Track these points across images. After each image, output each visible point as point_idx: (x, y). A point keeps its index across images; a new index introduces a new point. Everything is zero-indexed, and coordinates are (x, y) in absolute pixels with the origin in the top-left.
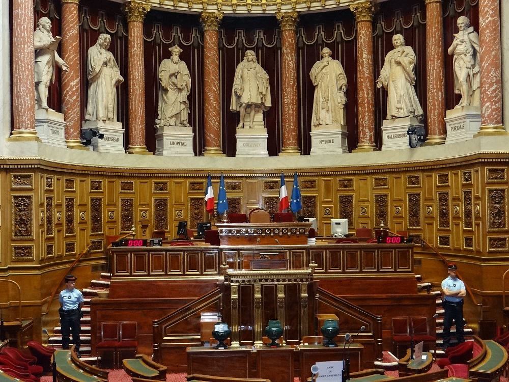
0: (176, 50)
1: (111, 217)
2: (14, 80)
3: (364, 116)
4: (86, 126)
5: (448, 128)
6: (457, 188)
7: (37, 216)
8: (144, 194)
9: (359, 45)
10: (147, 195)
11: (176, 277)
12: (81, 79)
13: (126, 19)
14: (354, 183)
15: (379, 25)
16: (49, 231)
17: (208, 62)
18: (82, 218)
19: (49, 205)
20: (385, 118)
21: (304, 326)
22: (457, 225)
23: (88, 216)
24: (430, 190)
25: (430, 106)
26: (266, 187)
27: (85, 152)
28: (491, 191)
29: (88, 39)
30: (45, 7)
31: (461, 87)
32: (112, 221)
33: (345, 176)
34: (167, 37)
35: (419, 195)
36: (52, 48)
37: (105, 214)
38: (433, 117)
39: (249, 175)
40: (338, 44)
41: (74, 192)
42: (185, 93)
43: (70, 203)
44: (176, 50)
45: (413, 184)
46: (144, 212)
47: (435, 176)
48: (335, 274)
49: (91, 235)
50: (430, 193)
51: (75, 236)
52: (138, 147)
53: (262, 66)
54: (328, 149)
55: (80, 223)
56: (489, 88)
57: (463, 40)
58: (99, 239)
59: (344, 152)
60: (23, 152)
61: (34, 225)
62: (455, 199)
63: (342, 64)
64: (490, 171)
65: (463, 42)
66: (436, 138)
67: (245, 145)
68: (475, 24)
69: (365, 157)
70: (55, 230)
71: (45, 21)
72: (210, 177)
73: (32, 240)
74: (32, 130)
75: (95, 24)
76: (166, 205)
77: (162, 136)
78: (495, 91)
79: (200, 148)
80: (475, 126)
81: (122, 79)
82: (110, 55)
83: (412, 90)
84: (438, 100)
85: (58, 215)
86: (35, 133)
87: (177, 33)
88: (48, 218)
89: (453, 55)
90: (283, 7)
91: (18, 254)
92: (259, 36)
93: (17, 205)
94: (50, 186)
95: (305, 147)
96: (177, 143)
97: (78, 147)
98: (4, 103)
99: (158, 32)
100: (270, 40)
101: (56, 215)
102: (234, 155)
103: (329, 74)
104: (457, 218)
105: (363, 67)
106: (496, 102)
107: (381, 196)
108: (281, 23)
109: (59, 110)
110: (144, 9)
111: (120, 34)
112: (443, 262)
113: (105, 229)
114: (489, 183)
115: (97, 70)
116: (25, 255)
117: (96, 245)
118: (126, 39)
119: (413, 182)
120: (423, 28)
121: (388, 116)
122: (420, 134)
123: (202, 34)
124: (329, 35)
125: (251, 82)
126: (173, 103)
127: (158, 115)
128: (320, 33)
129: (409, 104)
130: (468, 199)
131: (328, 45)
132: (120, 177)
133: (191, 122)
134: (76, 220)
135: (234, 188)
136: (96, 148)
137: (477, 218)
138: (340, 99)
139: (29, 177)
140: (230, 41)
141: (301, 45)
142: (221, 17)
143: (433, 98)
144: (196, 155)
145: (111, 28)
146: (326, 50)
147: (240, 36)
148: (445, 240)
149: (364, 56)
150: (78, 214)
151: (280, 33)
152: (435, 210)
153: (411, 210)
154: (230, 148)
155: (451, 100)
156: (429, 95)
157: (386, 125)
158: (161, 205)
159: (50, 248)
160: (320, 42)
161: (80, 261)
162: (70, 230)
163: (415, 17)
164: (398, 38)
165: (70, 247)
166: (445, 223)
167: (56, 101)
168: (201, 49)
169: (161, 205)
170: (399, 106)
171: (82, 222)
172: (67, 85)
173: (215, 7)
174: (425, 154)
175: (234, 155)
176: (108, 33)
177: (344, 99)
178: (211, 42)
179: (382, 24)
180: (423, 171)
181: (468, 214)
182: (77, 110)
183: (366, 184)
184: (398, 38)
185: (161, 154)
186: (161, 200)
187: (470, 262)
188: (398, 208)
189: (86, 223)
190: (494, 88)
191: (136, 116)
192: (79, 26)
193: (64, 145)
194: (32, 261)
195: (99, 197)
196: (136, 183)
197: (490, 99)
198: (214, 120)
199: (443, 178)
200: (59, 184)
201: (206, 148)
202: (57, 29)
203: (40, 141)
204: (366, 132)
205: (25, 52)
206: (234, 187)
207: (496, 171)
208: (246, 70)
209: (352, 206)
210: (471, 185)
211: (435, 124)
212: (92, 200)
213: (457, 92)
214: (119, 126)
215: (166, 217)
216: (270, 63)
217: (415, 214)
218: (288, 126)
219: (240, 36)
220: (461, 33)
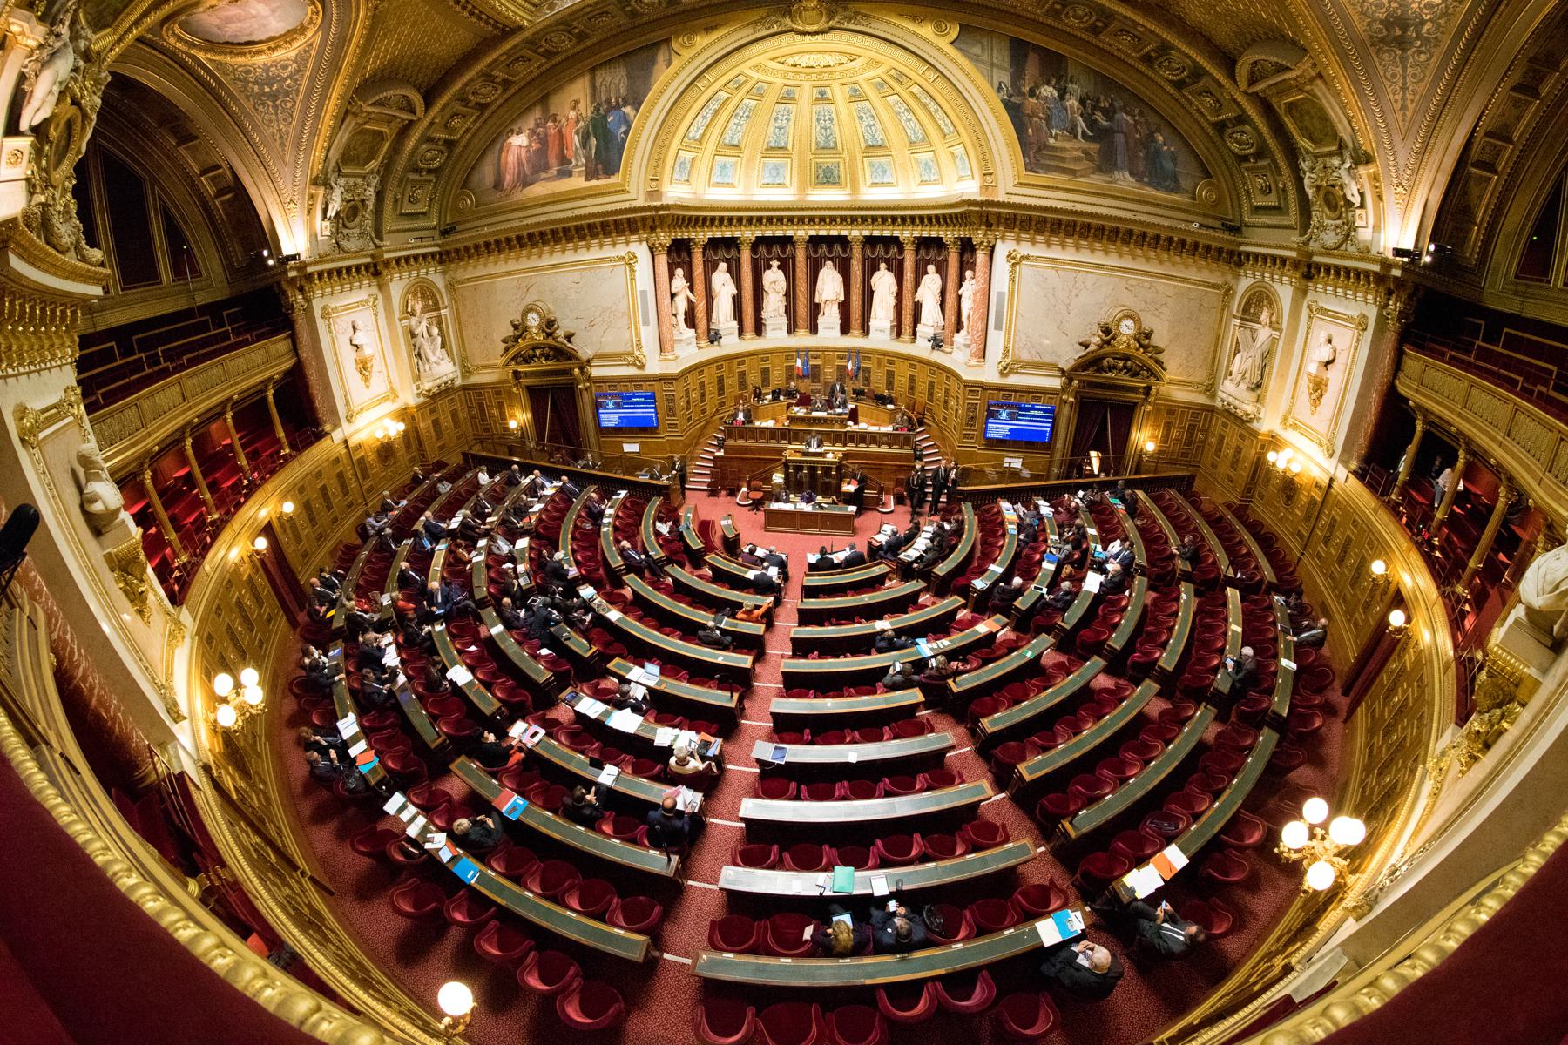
0: (775, 264)
3: (907, 317)
31: (964, 319)
33: (893, 357)
34: (769, 252)
37: (727, 382)
39: (824, 350)
43: (702, 385)
44: (775, 264)
52: (749, 334)
57: (968, 289)
66: (947, 348)
69: (904, 347)
71: (679, 272)
85: (694, 396)
87: (776, 249)
92: (837, 248)
95: (866, 330)
99: (762, 250)
100: (844, 251)
122: (937, 343)
125: (830, 284)
126: (774, 304)
131: (887, 262)
138: (893, 301)
140: (815, 252)
146: (883, 266)
147: (823, 248)
154: (814, 329)
155: (959, 326)
157: (920, 328)
158: (765, 372)
163: (944, 253)
164: (931, 268)
165: (704, 411)
167: (691, 321)
168: (794, 258)
174: (937, 357)
178: (801, 255)
179: (923, 251)
184: (931, 268)
188: (922, 387)
198: (802, 310)
202: (689, 277)
204: (907, 329)
214: (735, 324)
216: (844, 270)
217: (931, 394)
218: (854, 316)
219: (823, 248)
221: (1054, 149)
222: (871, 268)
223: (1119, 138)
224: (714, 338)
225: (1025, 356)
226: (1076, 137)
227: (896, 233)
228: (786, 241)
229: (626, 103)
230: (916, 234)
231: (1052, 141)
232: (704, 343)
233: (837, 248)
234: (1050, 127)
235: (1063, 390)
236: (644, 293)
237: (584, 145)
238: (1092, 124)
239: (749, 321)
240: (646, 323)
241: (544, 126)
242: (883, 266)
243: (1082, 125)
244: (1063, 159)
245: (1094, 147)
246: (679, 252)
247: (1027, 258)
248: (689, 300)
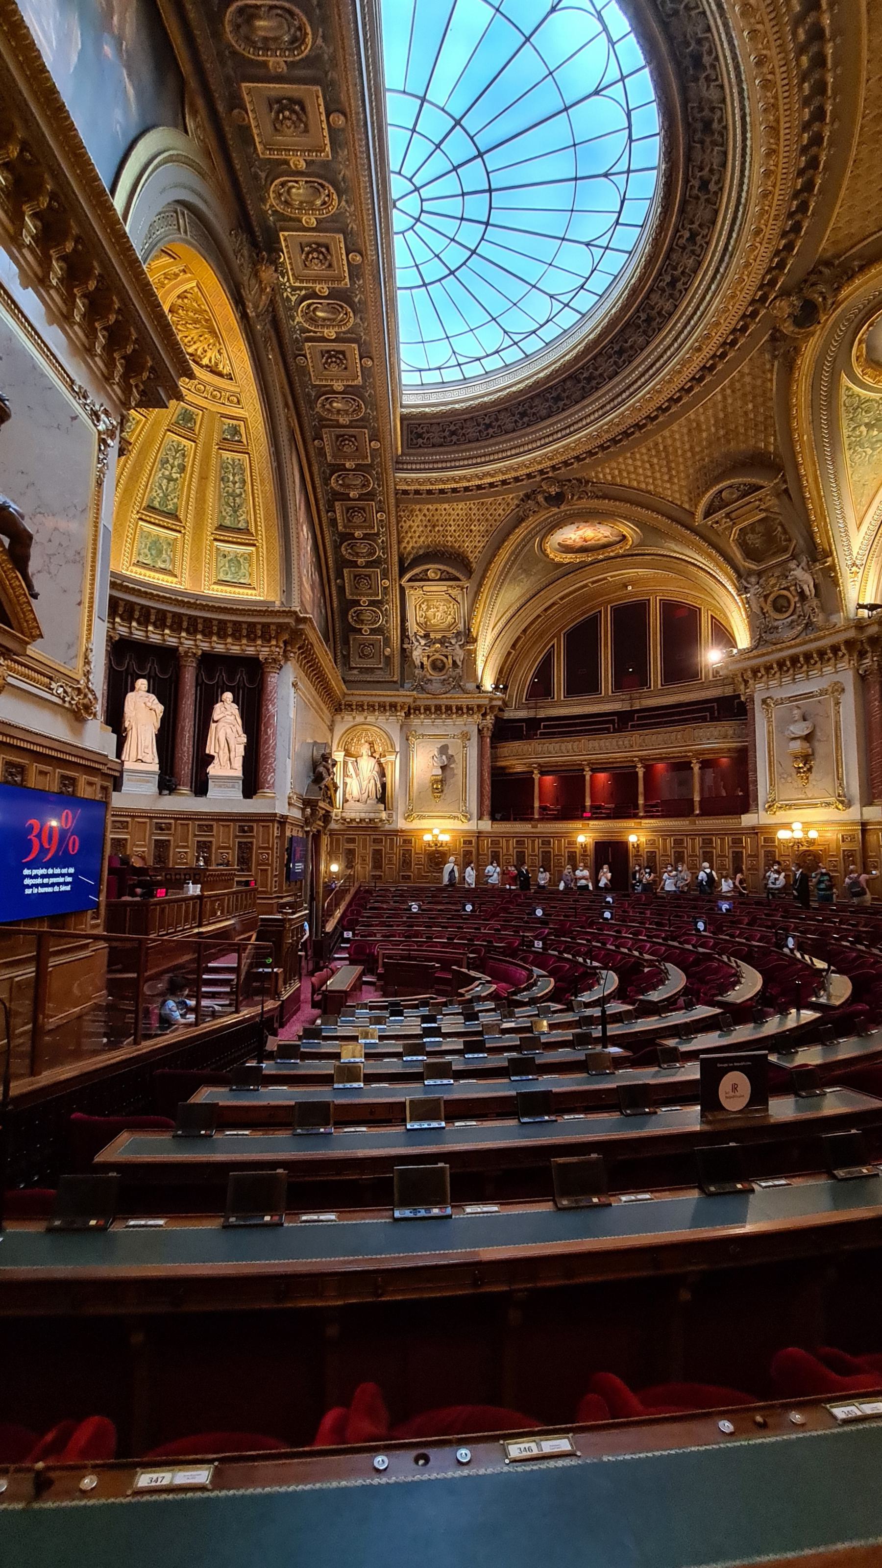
210: (253, 837)
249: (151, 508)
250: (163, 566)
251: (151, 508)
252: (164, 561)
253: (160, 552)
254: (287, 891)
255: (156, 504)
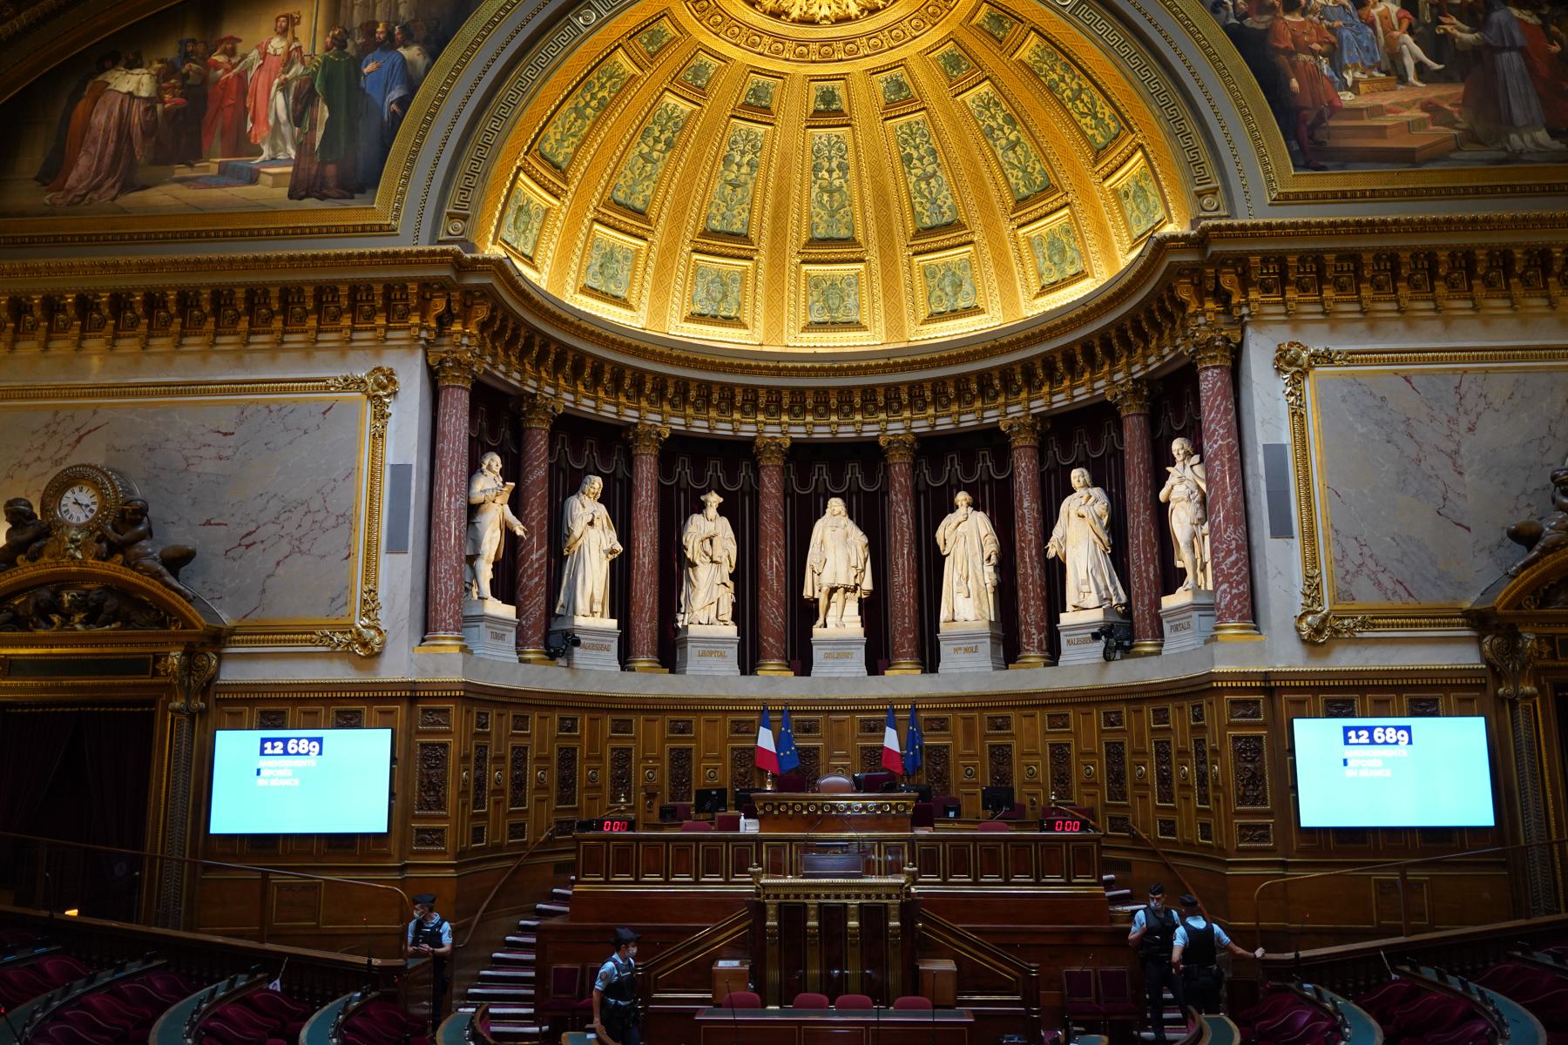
1: (591, 779)
2: (433, 553)
4: (556, 626)
5: (1166, 627)
6: (1183, 732)
7: (456, 776)
8: (649, 742)
9: (1016, 486)
10: (657, 744)
11: (681, 885)
12: (549, 551)
13: (630, 451)
14: (1013, 721)
15: (1050, 453)
16: (479, 802)
17: (765, 517)
18: (539, 780)
19: (481, 759)
20: (1064, 611)
21: (894, 977)
22: (1187, 799)
23: (551, 777)
24: (1141, 735)
25: (1135, 588)
26: (863, 729)
27: (550, 668)
28: (1236, 739)
29: (566, 484)
30: (494, 436)
31: (1184, 560)
32: (594, 786)
33: (995, 711)
34: (699, 478)
35: (1122, 744)
36: (499, 500)
37: (583, 772)
38: (1140, 609)
39: (832, 708)
40: (983, 484)
41: (528, 736)
42: (727, 569)
43: (520, 754)
44: (714, 500)
45: (1113, 724)
46: (651, 770)
47: (1148, 711)
48: (961, 886)
49: (557, 810)
50: (1141, 741)
51: (526, 811)
53: (859, 525)
54: (967, 668)
55: (537, 788)
56: (1224, 558)
58: (569, 817)
59: (995, 668)
60: (438, 671)
61: (451, 792)
62: (1182, 753)
63: (991, 519)
64: (1233, 702)
65: (1182, 480)
66: (1148, 646)
67: (827, 656)
68: (1198, 449)
69: (1032, 677)
70: (489, 801)
71: (494, 461)
72: (766, 712)
73: (445, 818)
74: (456, 634)
75: (578, 459)
76: (689, 759)
77: (685, 641)
78: (1235, 563)
79: (749, 661)
80: (1208, 623)
81: (619, 548)
82: (602, 510)
83: (1105, 565)
84: (1148, 578)
86: (461, 639)
87: (714, 470)
88: (477, 780)
89: (1168, 503)
90: (890, 426)
91: (422, 842)
92: (854, 474)
93: (424, 759)
94: (484, 726)
95: (929, 660)
96: (711, 654)
97: (537, 661)
98: (412, 590)
100: (870, 478)
101: (494, 775)
102: (809, 675)
103: (966, 537)
104: (1185, 786)
105: (1023, 523)
106: (1239, 583)
107: (1059, 746)
108: (886, 452)
109: (507, 599)
110: (659, 434)
111: (620, 475)
112: (1166, 865)
113: (581, 798)
114: (1231, 726)
115: (577, 533)
116: (433, 844)
117: (564, 827)
118: (630, 481)
119: (1112, 720)
120: (1118, 455)
121: (1069, 607)
122: (1119, 635)
123: (756, 469)
124: (969, 471)
125: (837, 550)
127: (680, 606)
128: (953, 466)
129: (1102, 586)
130: (1200, 753)
131: (970, 489)
132: (609, 710)
133: (735, 618)
134: (531, 783)
135: (807, 731)
136: (569, 665)
137: (1216, 787)
138: (989, 576)
139: (447, 711)
141: (922, 487)
142: (788, 443)
143: (1140, 576)
144: (743, 673)
145: (606, 463)
146: (962, 498)
147: (821, 474)
148: (1168, 827)
149: (1026, 504)
150: (533, 773)
151: (887, 467)
152: (1149, 770)
153: (1110, 771)
154: (801, 660)
155: (1171, 579)
156: (1133, 569)
157: (1065, 619)
158: (681, 759)
159: (478, 834)
160: (954, 481)
161: (532, 855)
162: (518, 800)
164: (1077, 476)
165: (516, 831)
166: (1166, 796)
168: (755, 495)
169: (681, 759)
170: (1085, 588)
171: (542, 787)
172: (524, 559)
173: (777, 429)
175: (809, 675)
176: (598, 474)
177: (994, 576)
178: (771, 485)
179: (1054, 451)
180: (1127, 701)
181: (1202, 778)
182: (541, 599)
183: (1034, 724)
185: (683, 672)
186: (681, 750)
187: (1209, 867)
189: (547, 789)
190: (1233, 558)
191: (642, 609)
192: (550, 465)
193: (514, 658)
194: (444, 853)
195: (574, 744)
196: (639, 722)
197: (1227, 578)
198: (773, 614)
199: (1161, 715)
200: (499, 725)
201: (762, 661)
203: (471, 652)
204: (1033, 635)
205: (451, 507)
206: (808, 728)
207: (1245, 703)
208: (828, 531)
209: (1010, 764)
210: (1203, 727)
211: (1144, 619)
212: (560, 749)
213: (1179, 564)
215: (690, 779)
216: (869, 517)
217: (1117, 778)
219: (821, 474)
220: (1179, 466)
221: (1356, 112)
222: (936, 507)
223: (1510, 61)
224: (558, 642)
225: (1368, 597)
226: (1403, 79)
227: (991, 416)
228: (740, 452)
229: (408, 40)
230: (1038, 406)
231: (1347, 97)
232: (531, 653)
233: (854, 474)
234: (1338, 67)
235: (1494, 671)
236: (401, 472)
237: (300, 112)
238: (1436, 44)
239: (645, 626)
240: (397, 545)
241: (204, 60)
242: (962, 498)
243: (1412, 51)
244: (1381, 131)
245: (1448, 94)
246: (497, 422)
247: (1327, 358)
248: (508, 533)
249: (1021, 202)
250: (1073, 271)
251: (1021, 202)
252: (1072, 263)
253: (1063, 251)
254: (1301, 852)
255: (1024, 191)
